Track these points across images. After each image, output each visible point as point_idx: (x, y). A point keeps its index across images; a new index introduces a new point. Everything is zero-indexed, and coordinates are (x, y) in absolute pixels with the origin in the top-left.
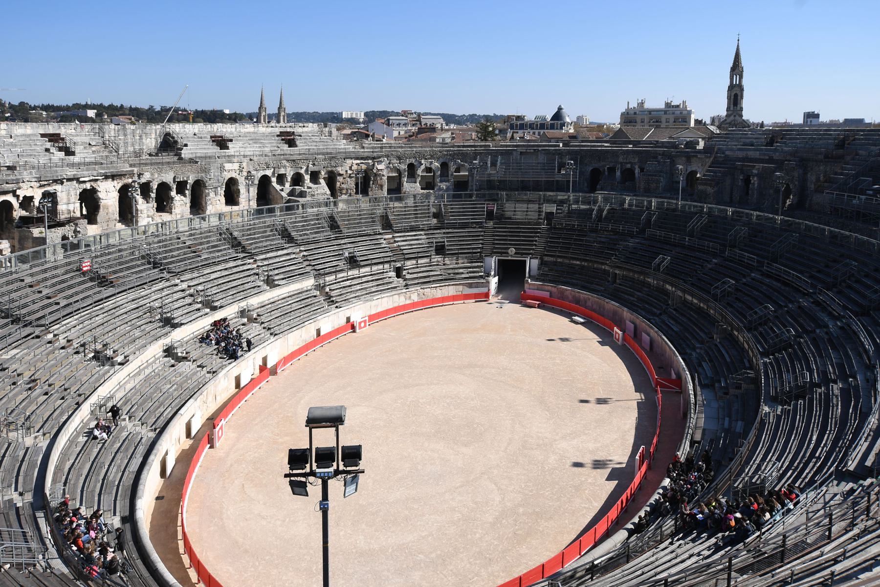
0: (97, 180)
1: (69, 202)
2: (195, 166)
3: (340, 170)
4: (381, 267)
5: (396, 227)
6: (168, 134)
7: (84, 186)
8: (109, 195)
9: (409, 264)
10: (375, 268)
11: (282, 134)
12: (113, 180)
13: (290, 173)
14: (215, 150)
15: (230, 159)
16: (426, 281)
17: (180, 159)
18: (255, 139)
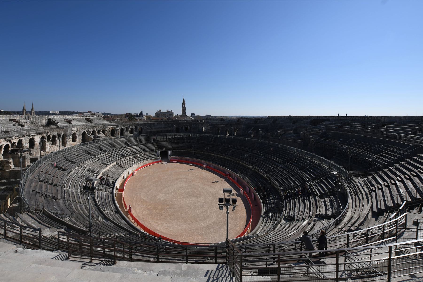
1: (26, 144)
2: (63, 129)
5: (131, 145)
6: (51, 119)
7: (30, 137)
8: (37, 139)
9: (138, 155)
11: (86, 119)
13: (91, 131)
14: (68, 124)
15: (74, 127)
16: (144, 159)
18: (79, 120)
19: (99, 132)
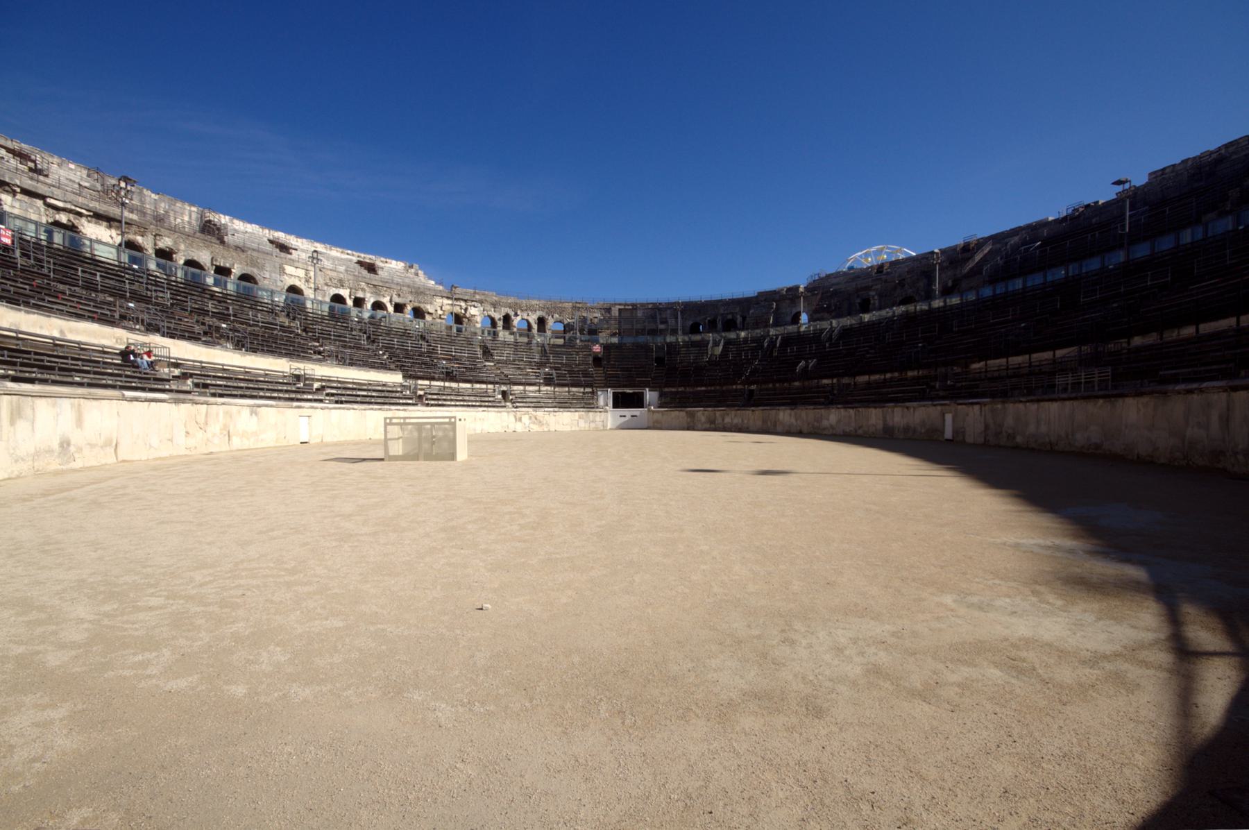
0: (80, 215)
3: (430, 308)
4: (484, 386)
9: (518, 389)
10: (478, 386)
12: (110, 227)
17: (222, 242)
19: (399, 308)
